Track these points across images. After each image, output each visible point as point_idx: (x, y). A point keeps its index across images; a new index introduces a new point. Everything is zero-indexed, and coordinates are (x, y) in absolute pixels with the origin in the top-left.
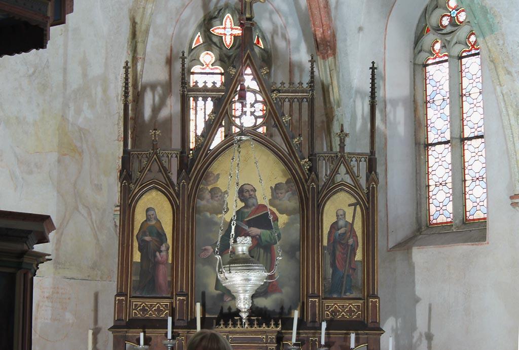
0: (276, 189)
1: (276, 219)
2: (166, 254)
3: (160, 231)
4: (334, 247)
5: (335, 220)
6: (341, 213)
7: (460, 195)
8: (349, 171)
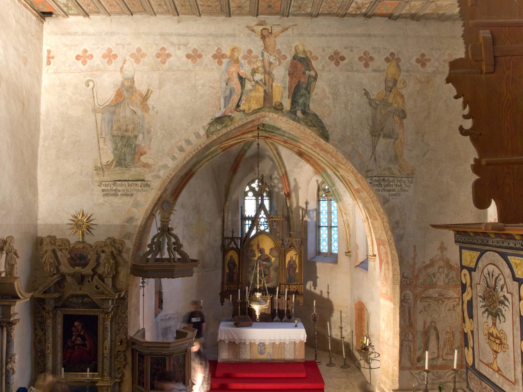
2: (236, 271)
7: (330, 244)
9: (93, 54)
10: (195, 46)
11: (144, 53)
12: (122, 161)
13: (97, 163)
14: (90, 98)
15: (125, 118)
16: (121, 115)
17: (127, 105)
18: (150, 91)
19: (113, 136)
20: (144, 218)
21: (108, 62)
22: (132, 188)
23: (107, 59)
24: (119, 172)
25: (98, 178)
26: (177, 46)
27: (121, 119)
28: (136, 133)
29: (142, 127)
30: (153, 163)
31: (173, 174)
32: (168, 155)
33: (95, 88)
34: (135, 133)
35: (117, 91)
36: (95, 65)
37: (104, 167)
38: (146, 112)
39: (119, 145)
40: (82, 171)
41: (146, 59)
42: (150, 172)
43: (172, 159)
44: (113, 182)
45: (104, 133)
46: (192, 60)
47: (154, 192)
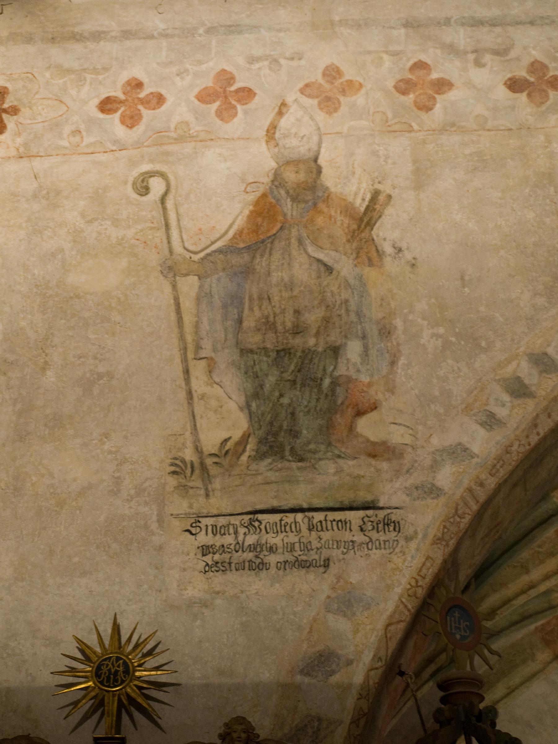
9: (163, 92)
10: (536, 54)
11: (350, 82)
12: (281, 439)
13: (180, 449)
14: (151, 228)
15: (290, 286)
16: (275, 277)
17: (294, 241)
18: (382, 198)
19: (244, 352)
20: (377, 658)
21: (219, 114)
22: (326, 535)
23: (218, 103)
24: (272, 476)
25: (185, 504)
26: (471, 57)
27: (274, 292)
28: (334, 337)
29: (359, 314)
30: (408, 440)
31: (492, 483)
32: (468, 409)
33: (171, 196)
34: (332, 338)
35: (257, 203)
36: (172, 126)
37: (209, 461)
38: (371, 264)
39: (270, 381)
40: (118, 481)
41: (360, 99)
42: (398, 473)
43: (483, 424)
44: (247, 518)
45: (207, 344)
46: (529, 95)
47: (418, 550)
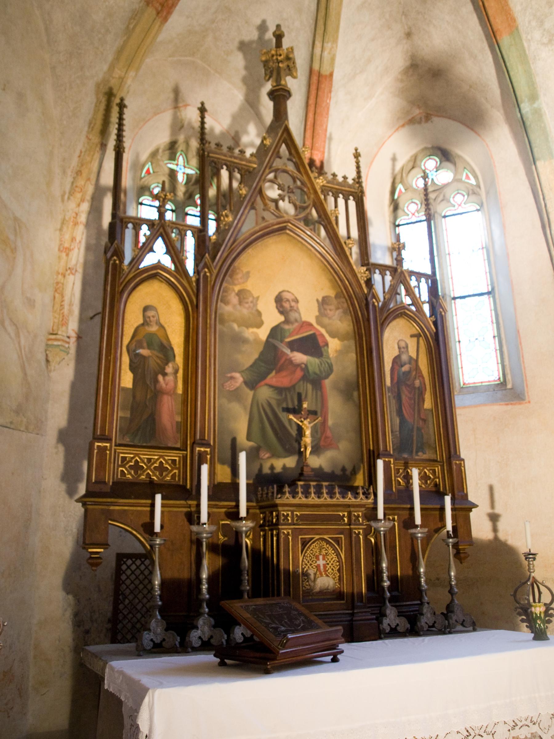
0: (324, 302)
1: (327, 345)
3: (165, 342)
4: (399, 390)
5: (396, 353)
6: (403, 344)
8: (409, 292)
